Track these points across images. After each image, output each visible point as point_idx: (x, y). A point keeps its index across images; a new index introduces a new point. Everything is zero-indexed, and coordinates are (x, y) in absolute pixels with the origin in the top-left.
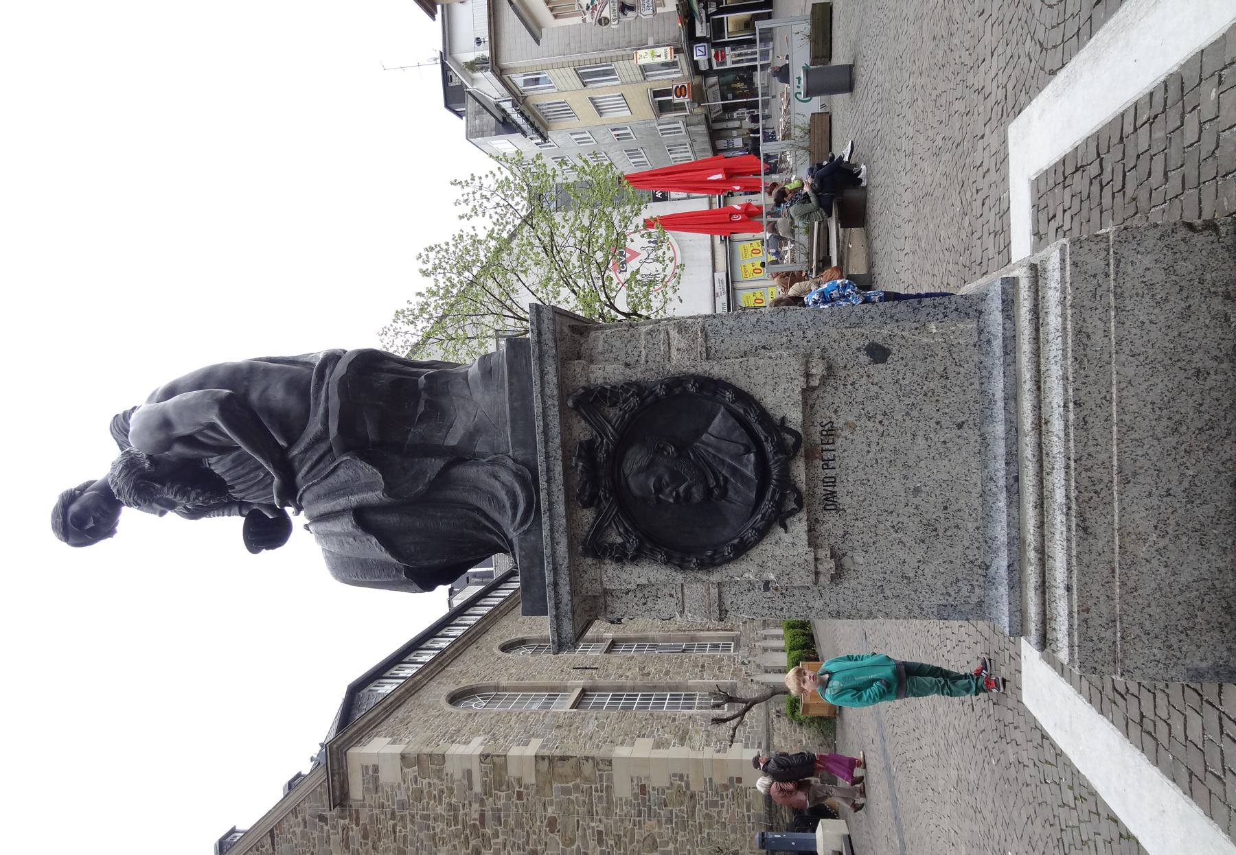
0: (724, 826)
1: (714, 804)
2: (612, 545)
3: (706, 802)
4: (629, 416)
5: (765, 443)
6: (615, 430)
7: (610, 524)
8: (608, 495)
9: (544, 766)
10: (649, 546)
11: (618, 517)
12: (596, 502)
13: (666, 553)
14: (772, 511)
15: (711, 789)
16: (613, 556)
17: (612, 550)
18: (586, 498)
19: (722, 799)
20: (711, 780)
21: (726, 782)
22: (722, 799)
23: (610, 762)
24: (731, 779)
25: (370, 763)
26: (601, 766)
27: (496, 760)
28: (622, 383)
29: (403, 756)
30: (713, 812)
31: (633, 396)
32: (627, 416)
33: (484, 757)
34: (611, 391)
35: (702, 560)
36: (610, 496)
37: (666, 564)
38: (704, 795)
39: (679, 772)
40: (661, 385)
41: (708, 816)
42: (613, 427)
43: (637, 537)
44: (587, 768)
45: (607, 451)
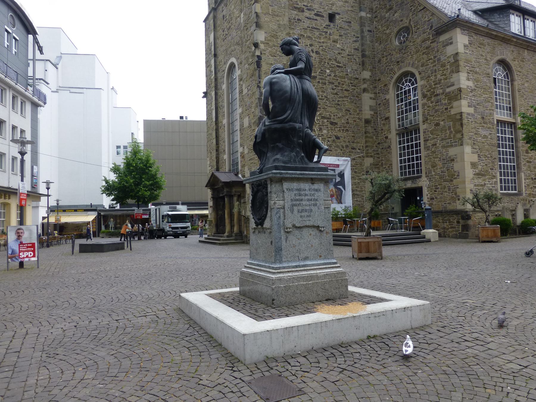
0: (442, 194)
1: (449, 190)
3: (450, 186)
9: (458, 117)
15: (454, 188)
19: (451, 193)
20: (458, 188)
21: (458, 194)
22: (451, 193)
23: (462, 145)
24: (459, 196)
25: (454, 40)
26: (460, 141)
27: (459, 96)
29: (457, 54)
30: (446, 190)
33: (460, 90)
38: (452, 185)
39: (460, 174)
41: (445, 187)
44: (459, 136)
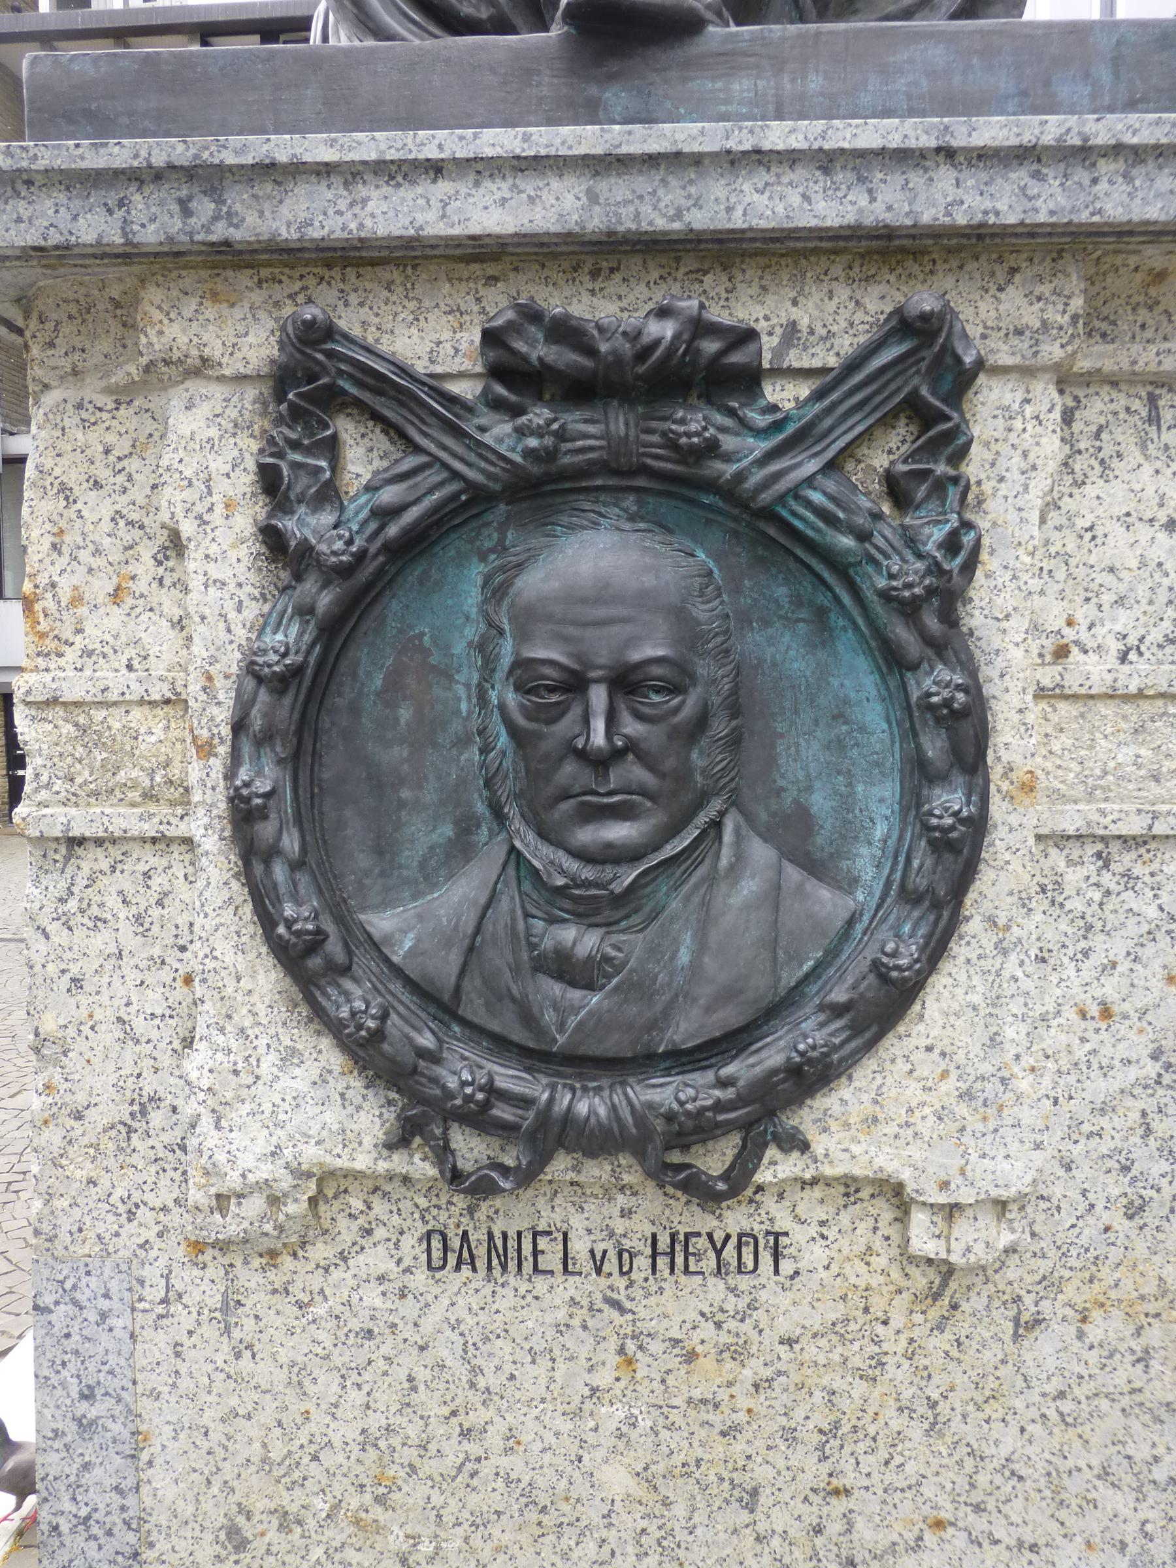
2: (332, 447)
4: (848, 551)
5: (710, 1076)
6: (795, 492)
7: (418, 449)
8: (533, 442)
10: (325, 600)
11: (441, 484)
12: (500, 390)
13: (297, 671)
14: (449, 1095)
16: (280, 455)
17: (309, 451)
18: (520, 346)
28: (983, 524)
31: (928, 572)
32: (847, 542)
34: (955, 480)
35: (262, 814)
36: (529, 453)
37: (252, 670)
40: (958, 687)
42: (809, 481)
43: (361, 557)
45: (711, 449)
